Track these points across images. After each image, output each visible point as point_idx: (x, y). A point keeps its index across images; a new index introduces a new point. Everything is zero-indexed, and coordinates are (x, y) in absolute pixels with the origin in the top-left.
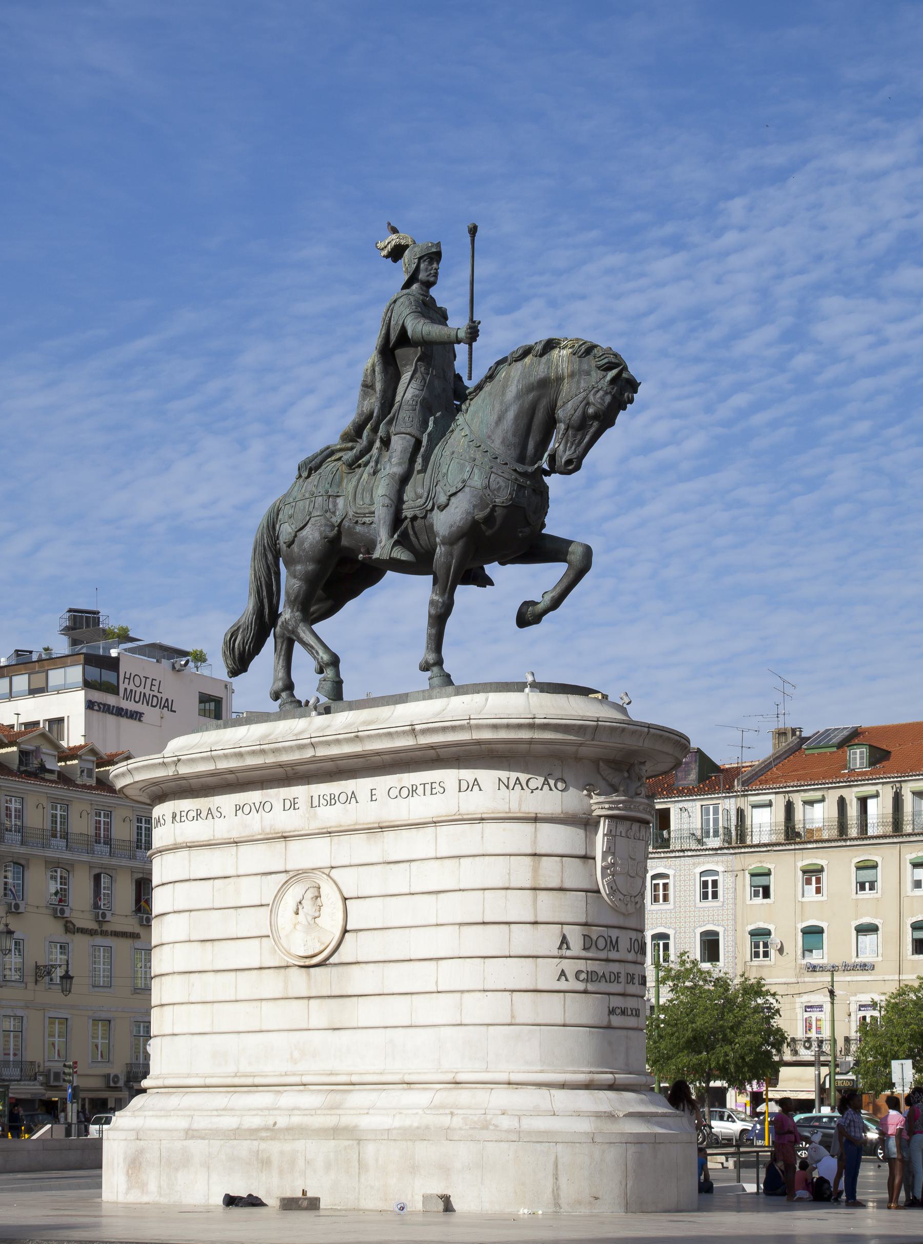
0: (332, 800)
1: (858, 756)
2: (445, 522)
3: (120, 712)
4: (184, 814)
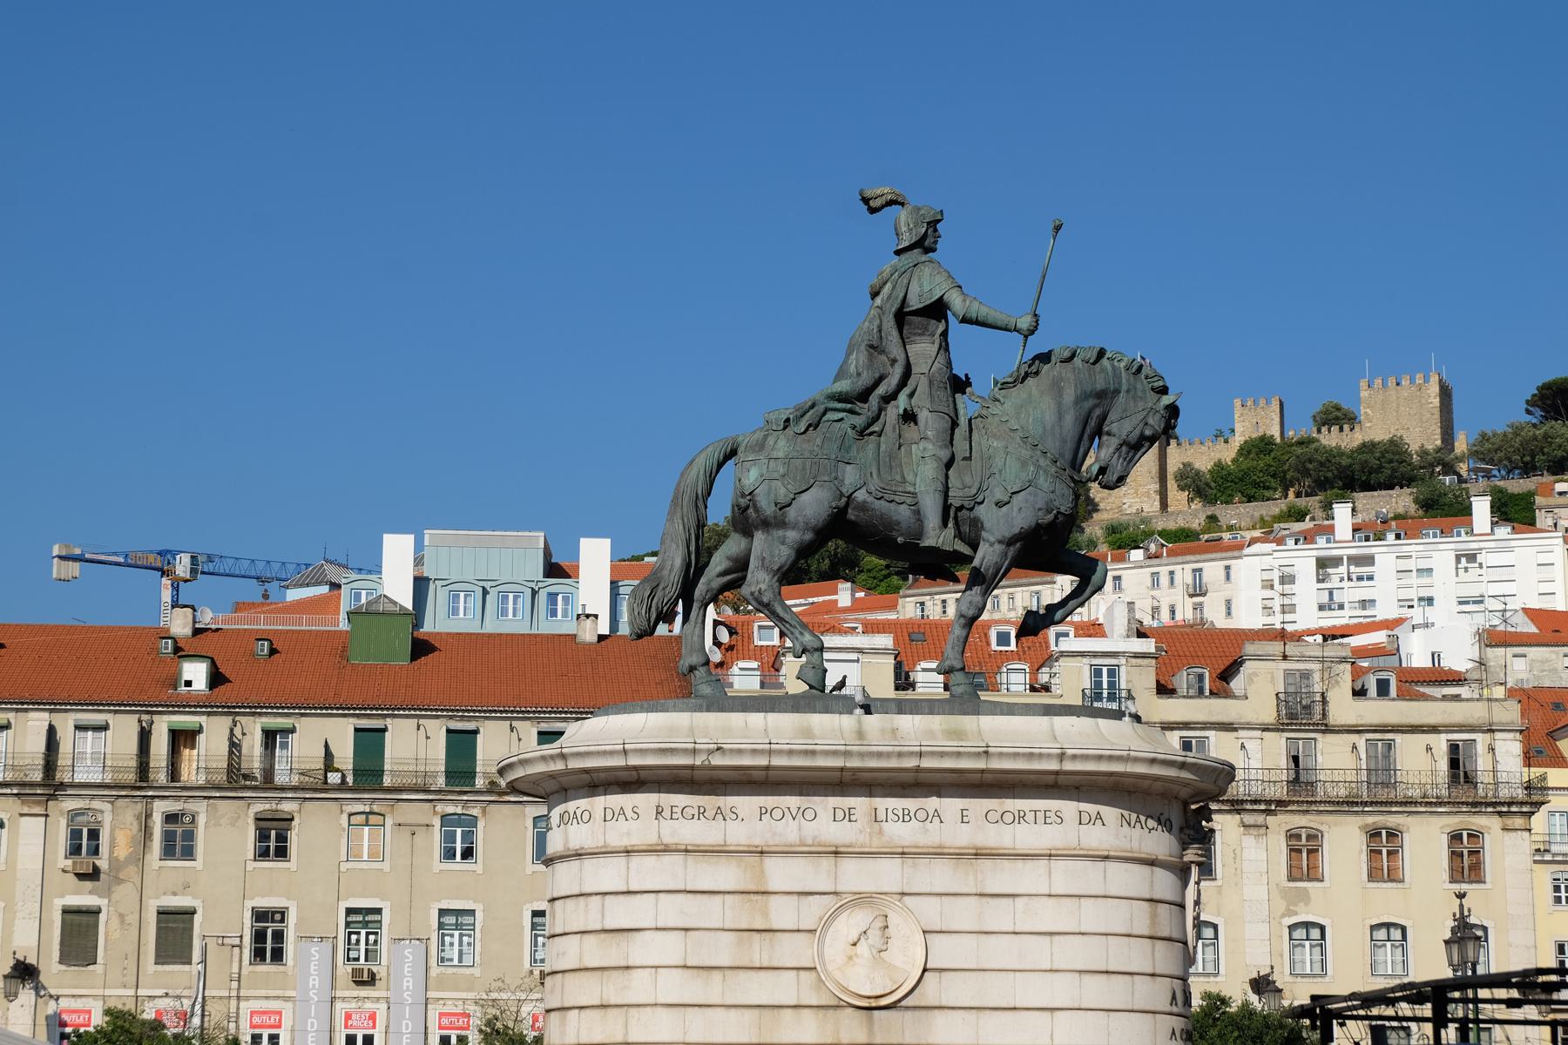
0: (906, 816)
4: (678, 810)
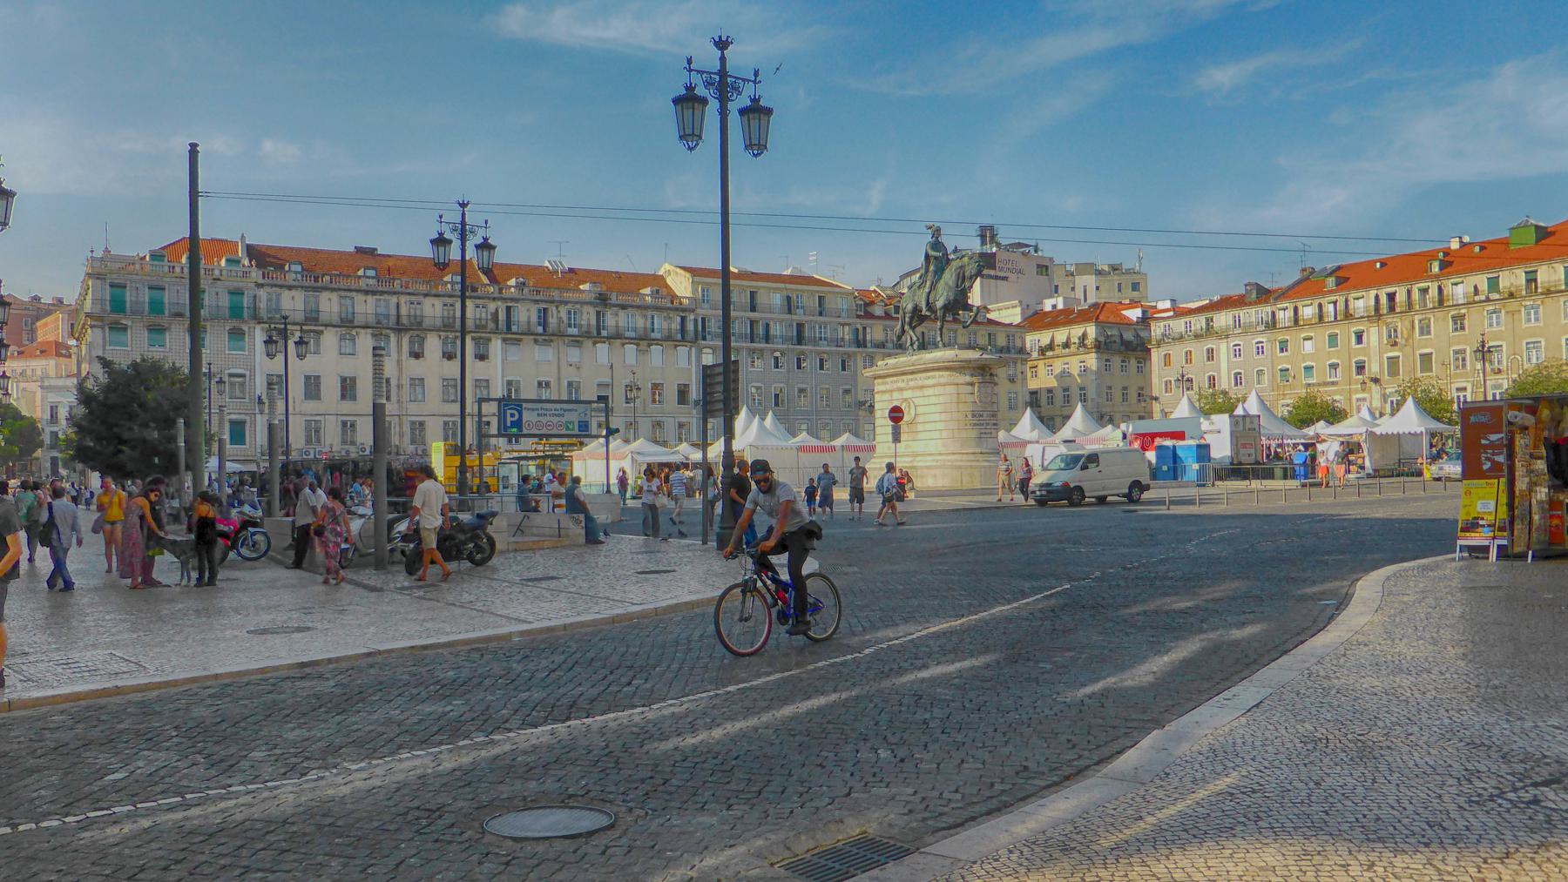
1: (1331, 281)
2: (939, 304)
3: (997, 278)
